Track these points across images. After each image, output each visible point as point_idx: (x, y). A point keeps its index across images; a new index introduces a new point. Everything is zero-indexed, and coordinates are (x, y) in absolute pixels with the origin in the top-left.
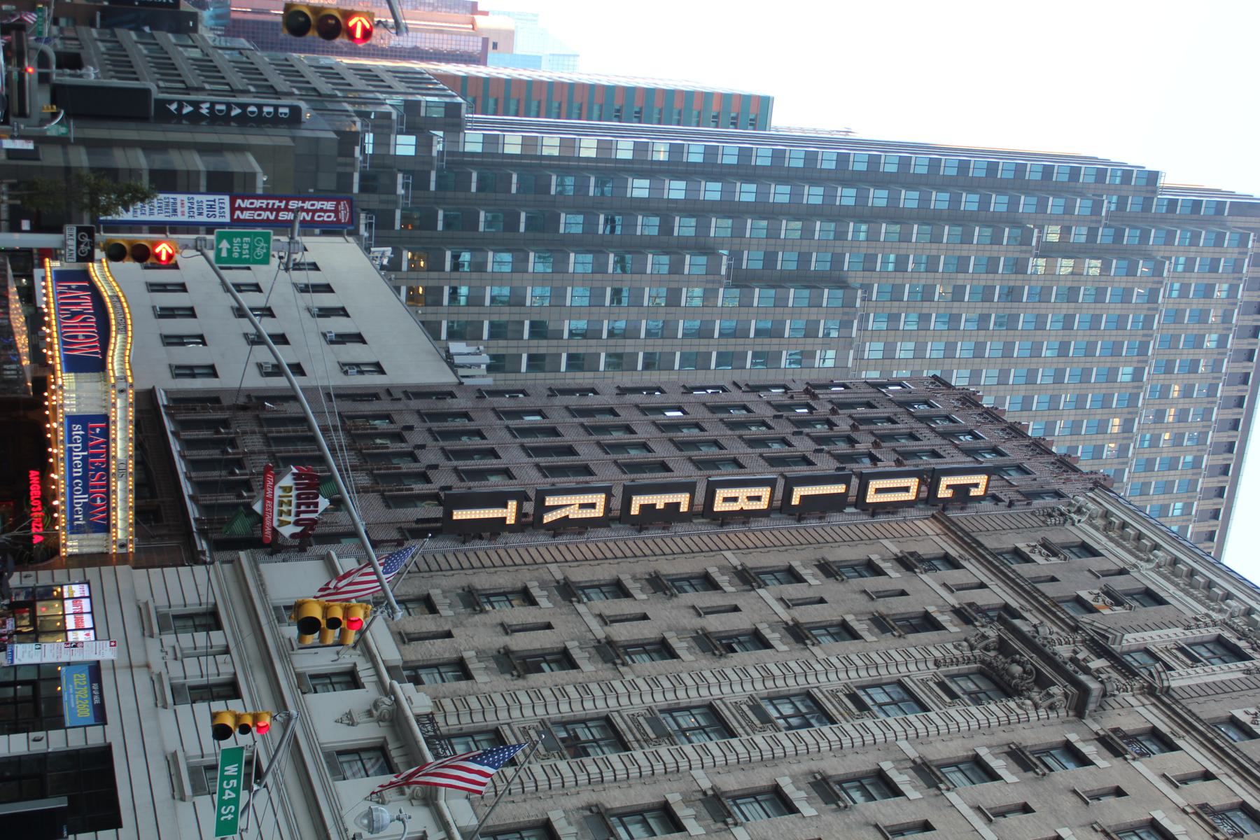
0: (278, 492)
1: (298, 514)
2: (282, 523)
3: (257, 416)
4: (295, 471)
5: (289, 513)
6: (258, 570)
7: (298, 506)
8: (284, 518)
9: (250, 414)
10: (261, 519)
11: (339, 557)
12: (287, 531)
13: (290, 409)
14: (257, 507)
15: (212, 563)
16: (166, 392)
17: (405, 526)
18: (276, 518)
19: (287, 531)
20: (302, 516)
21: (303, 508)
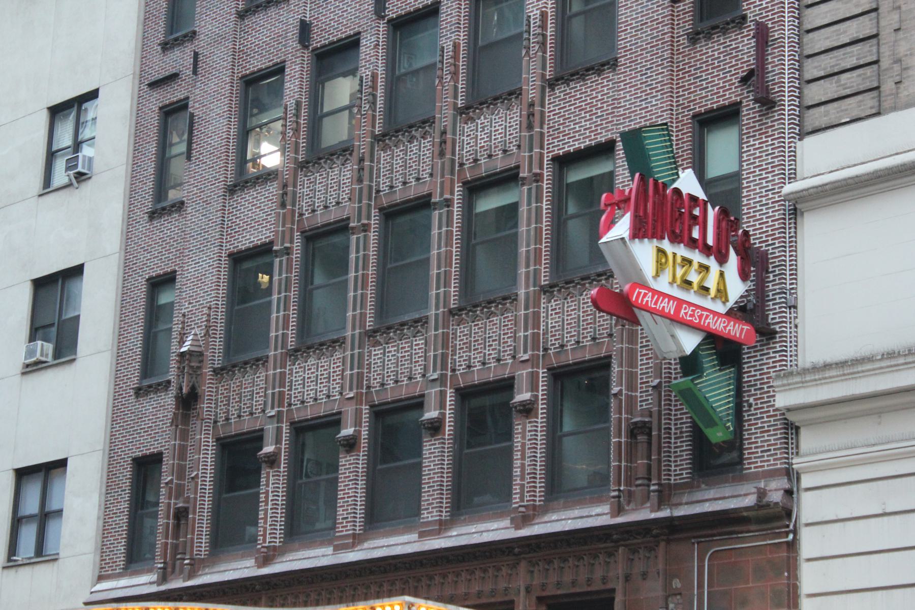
0: (663, 285)
1: (707, 250)
2: (722, 293)
3: (216, 372)
4: (622, 227)
5: (704, 268)
6: (805, 371)
7: (692, 244)
8: (712, 282)
9: (208, 387)
10: (712, 339)
11: (793, 177)
12: (736, 288)
13: (201, 295)
14: (689, 342)
15: (790, 473)
16: (101, 578)
17: (686, 24)
18: (707, 303)
19: (736, 288)
20: (710, 241)
21: (696, 234)
